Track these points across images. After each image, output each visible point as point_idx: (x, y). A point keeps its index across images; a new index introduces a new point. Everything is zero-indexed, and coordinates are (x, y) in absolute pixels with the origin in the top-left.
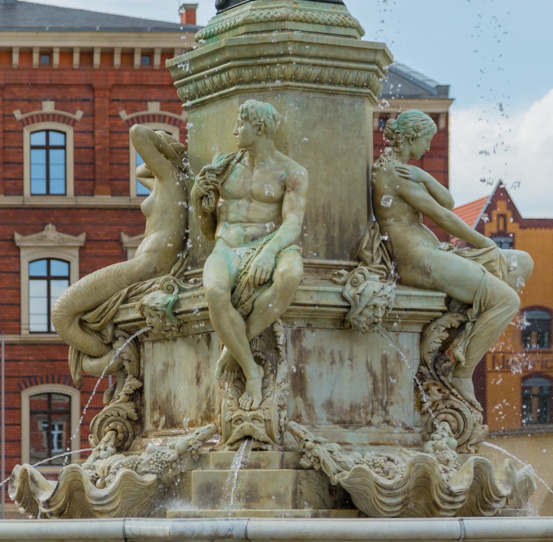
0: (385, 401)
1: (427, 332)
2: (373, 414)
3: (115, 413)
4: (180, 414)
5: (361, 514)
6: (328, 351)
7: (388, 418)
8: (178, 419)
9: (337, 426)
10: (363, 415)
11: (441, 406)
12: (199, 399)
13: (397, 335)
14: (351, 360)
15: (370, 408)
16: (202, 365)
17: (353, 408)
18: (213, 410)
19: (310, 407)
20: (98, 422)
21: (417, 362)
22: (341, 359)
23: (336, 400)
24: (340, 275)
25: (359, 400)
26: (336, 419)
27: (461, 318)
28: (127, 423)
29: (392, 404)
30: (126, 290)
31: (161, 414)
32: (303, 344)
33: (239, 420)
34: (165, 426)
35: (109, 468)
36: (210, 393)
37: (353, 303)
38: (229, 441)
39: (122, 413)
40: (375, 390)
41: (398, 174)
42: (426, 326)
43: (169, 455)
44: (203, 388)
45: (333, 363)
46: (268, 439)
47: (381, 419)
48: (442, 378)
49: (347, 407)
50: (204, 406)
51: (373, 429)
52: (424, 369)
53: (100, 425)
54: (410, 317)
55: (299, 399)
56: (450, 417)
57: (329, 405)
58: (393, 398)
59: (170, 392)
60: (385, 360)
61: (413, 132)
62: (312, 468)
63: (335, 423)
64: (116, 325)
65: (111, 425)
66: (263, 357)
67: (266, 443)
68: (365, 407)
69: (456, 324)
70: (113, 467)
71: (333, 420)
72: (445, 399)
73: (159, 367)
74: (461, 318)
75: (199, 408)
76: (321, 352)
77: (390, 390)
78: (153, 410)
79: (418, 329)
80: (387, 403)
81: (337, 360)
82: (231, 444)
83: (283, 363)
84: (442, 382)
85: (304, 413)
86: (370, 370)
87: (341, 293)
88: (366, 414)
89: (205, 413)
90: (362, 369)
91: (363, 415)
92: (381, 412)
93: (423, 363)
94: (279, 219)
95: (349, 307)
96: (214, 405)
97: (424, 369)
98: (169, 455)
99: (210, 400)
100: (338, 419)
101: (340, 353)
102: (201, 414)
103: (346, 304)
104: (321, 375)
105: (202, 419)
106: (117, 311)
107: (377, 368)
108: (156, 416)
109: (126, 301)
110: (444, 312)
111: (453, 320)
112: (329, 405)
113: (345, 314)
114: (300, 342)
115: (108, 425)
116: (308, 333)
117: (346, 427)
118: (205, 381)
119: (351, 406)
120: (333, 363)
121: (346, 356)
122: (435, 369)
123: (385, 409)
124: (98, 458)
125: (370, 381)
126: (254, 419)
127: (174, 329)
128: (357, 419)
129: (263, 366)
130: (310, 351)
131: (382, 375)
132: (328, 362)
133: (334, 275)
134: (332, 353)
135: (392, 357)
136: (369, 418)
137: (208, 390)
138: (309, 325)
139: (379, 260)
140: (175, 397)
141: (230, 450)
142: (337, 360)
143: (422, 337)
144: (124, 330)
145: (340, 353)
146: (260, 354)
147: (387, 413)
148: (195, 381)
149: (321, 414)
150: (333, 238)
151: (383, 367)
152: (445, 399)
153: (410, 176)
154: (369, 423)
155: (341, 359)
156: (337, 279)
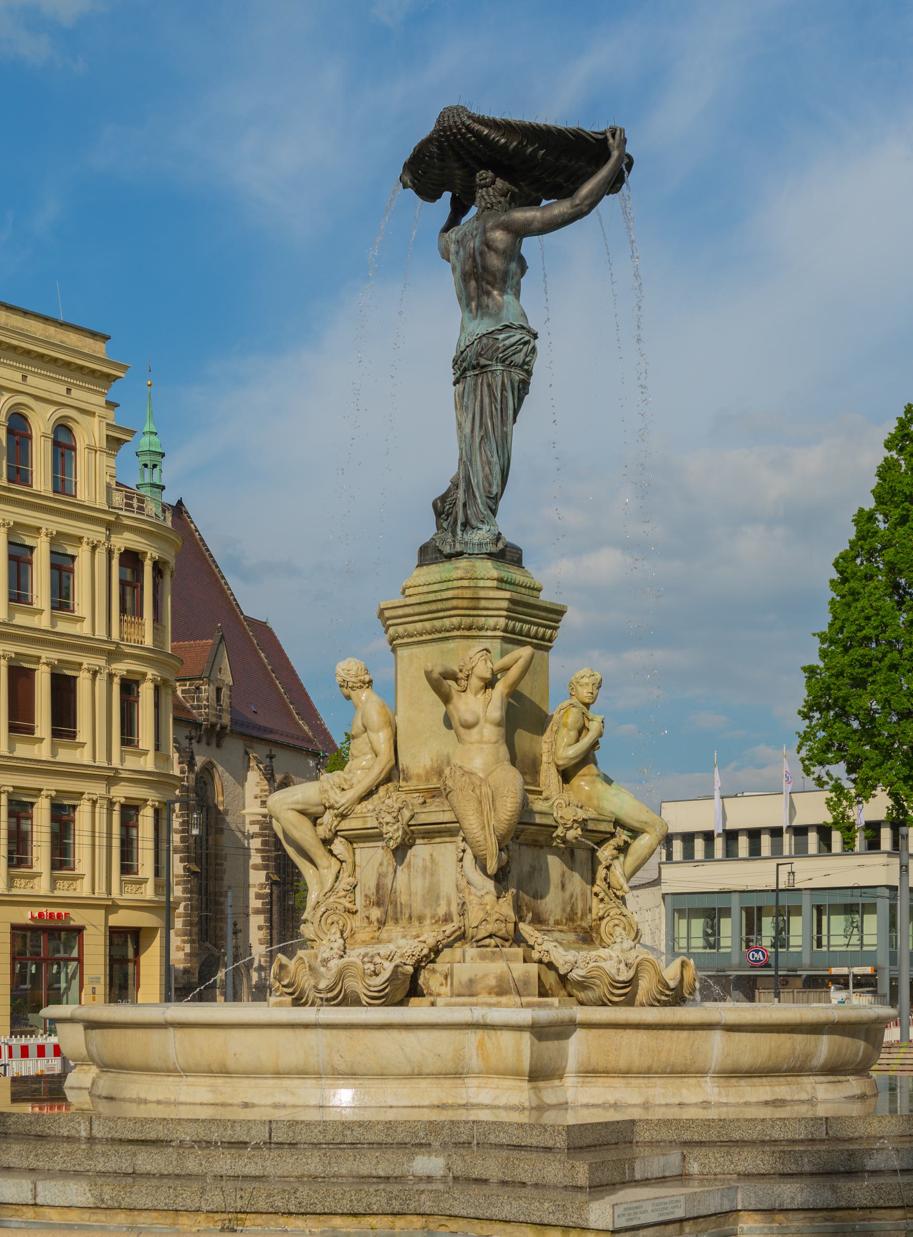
4: (546, 913)
8: (545, 916)
12: (564, 902)
16: (566, 874)
18: (576, 914)
36: (574, 899)
44: (567, 894)
50: (568, 909)
59: (537, 892)
73: (526, 868)
75: (564, 910)
89: (569, 914)
96: (577, 909)
99: (573, 904)
102: (566, 915)
105: (567, 920)
118: (569, 888)
137: (572, 896)
148: (560, 886)
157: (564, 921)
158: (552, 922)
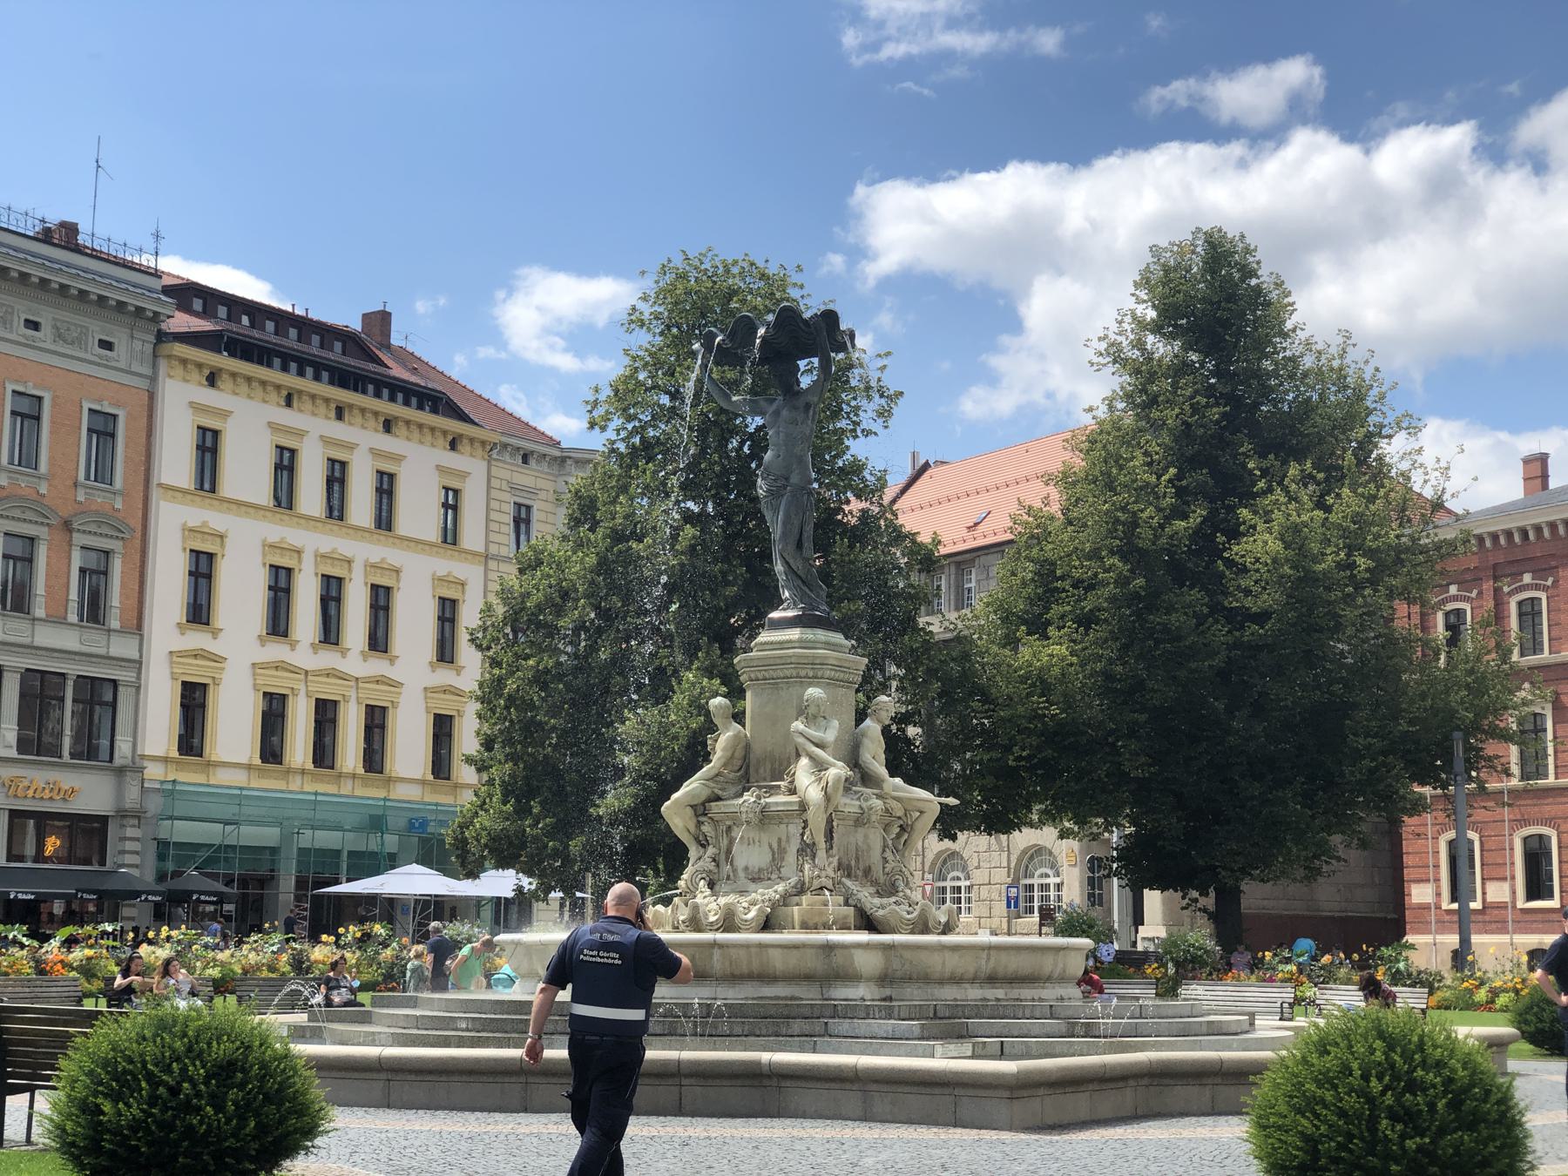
17: (760, 870)
19: (735, 871)
23: (750, 866)
25: (763, 866)
40: (774, 859)
49: (756, 870)
57: (746, 868)
60: (780, 840)
77: (782, 859)
85: (731, 874)
86: (770, 847)
107: (775, 846)
112: (746, 868)
116: (735, 828)
123: (779, 870)
125: (770, 855)
135: (784, 838)
149: (741, 874)
154: (769, 879)
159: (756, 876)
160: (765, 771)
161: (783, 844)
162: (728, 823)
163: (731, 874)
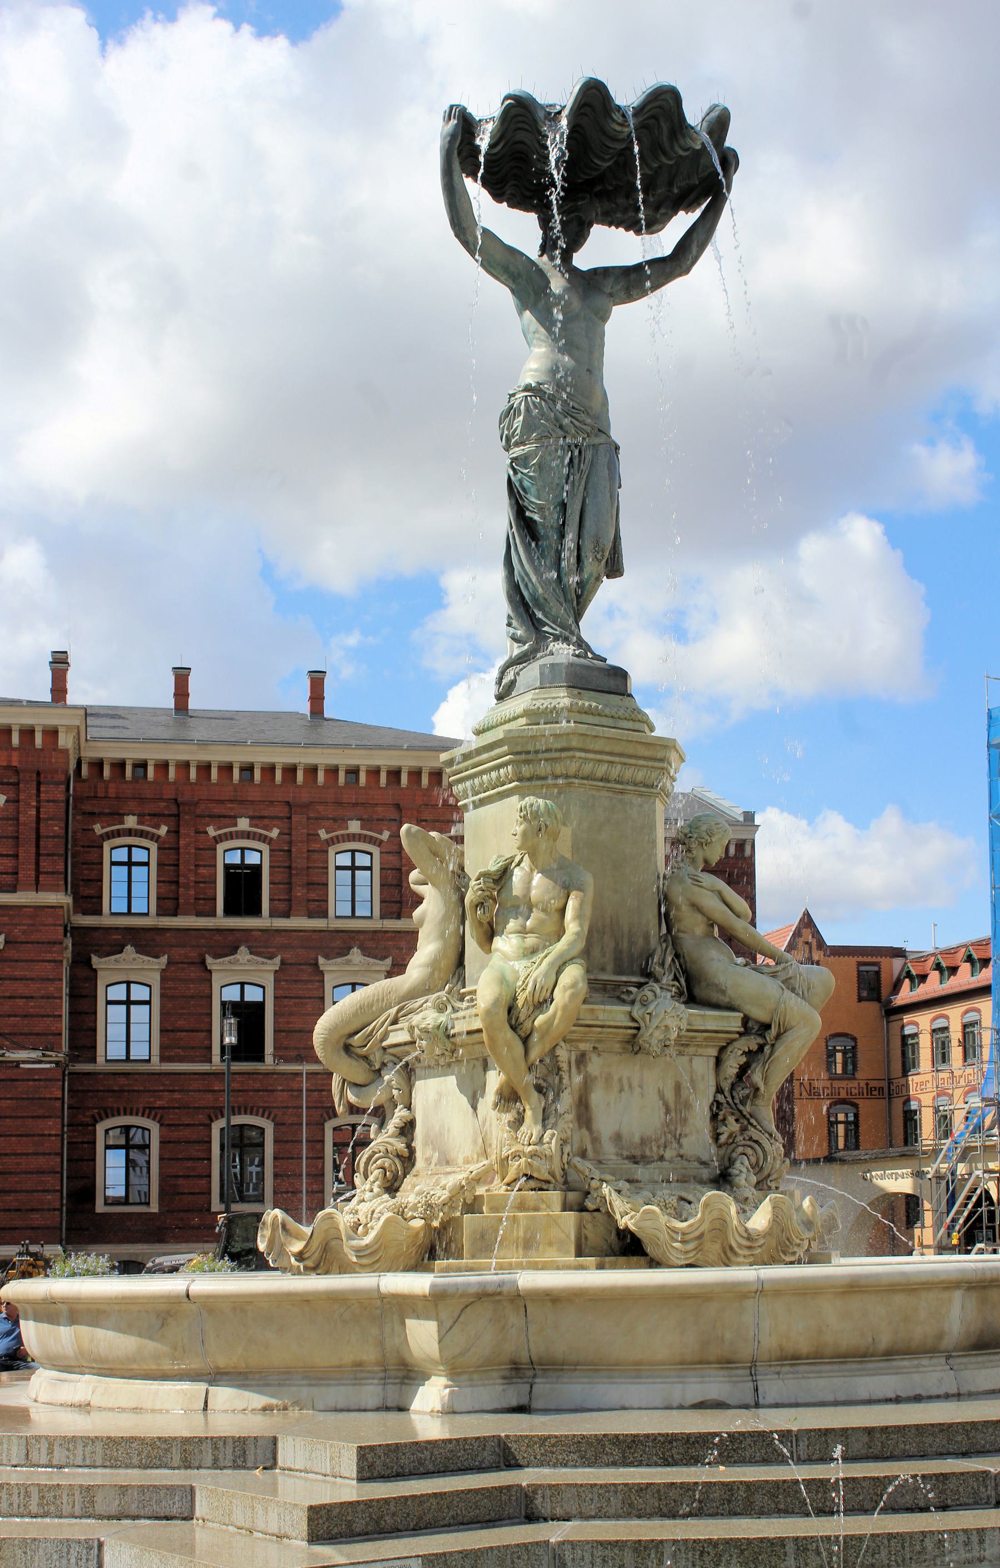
0: (678, 1132)
1: (724, 1057)
2: (665, 1147)
3: (382, 1149)
5: (654, 1263)
6: (616, 1078)
7: (682, 1152)
9: (627, 1162)
10: (655, 1149)
11: (739, 1138)
13: (691, 1060)
14: (641, 1087)
15: (663, 1141)
17: (644, 1142)
19: (595, 1140)
20: (364, 1160)
21: (713, 1089)
22: (630, 1086)
24: (629, 992)
26: (625, 1153)
27: (760, 1041)
28: (397, 1161)
29: (686, 1136)
30: (393, 1011)
31: (434, 1150)
32: (588, 1069)
33: (517, 1156)
34: (439, 1163)
35: (373, 1212)
36: (487, 1124)
37: (642, 1024)
38: (506, 1180)
39: (390, 1148)
41: (690, 881)
42: (722, 1049)
43: (439, 1198)
45: (621, 1090)
46: (550, 1178)
47: (674, 1153)
48: (741, 1107)
49: (637, 1139)
51: (665, 1164)
52: (720, 1098)
53: (367, 1164)
54: (706, 1039)
55: (584, 1131)
56: (749, 1151)
57: (618, 1138)
58: (687, 1130)
60: (678, 1088)
61: (707, 837)
62: (598, 1210)
63: (624, 1159)
64: (384, 1049)
65: (379, 1162)
66: (544, 1084)
67: (548, 1182)
68: (657, 1140)
69: (754, 1047)
70: (377, 1211)
71: (622, 1155)
72: (743, 1129)
74: (760, 1041)
75: (475, 1142)
76: (608, 1079)
77: (684, 1121)
78: (425, 1144)
79: (714, 1052)
80: (680, 1135)
81: (626, 1087)
82: (508, 1185)
83: (566, 1092)
84: (740, 1111)
85: (589, 1148)
86: (662, 1097)
87: (630, 1013)
88: (659, 1147)
90: (653, 1098)
91: (655, 1149)
92: (675, 1145)
93: (719, 1090)
94: (561, 932)
95: (638, 1029)
97: (720, 1098)
98: (439, 1198)
100: (628, 1153)
101: (629, 1079)
103: (636, 1025)
104: (608, 1104)
106: (385, 1036)
107: (670, 1095)
108: (429, 1152)
109: (395, 1022)
110: (741, 1034)
111: (752, 1043)
112: (618, 1138)
113: (635, 1036)
114: (585, 1067)
115: (375, 1162)
117: (636, 1163)
119: (642, 1139)
120: (621, 1090)
121: (635, 1083)
122: (733, 1098)
124: (363, 1201)
126: (533, 1155)
127: (447, 1053)
128: (648, 1153)
129: (544, 1095)
130: (596, 1078)
131: (676, 1103)
132: (616, 1089)
133: (623, 993)
134: (620, 1080)
135: (686, 1084)
136: (661, 1152)
138: (595, 1048)
139: (671, 977)
140: (449, 1131)
141: (507, 1190)
142: (626, 1087)
143: (718, 1062)
144: (394, 1055)
145: (629, 1079)
146: (541, 1082)
147: (681, 1146)
149: (609, 1150)
150: (621, 952)
151: (676, 1095)
152: (743, 1129)
153: (703, 884)
154: (661, 1158)
155: (630, 1086)
156: (623, 996)
157: (475, 1156)
158: (460, 1161)
159: (638, 1153)
160: (604, 955)
161: (684, 1093)
162: (583, 1046)
163: (589, 1148)
